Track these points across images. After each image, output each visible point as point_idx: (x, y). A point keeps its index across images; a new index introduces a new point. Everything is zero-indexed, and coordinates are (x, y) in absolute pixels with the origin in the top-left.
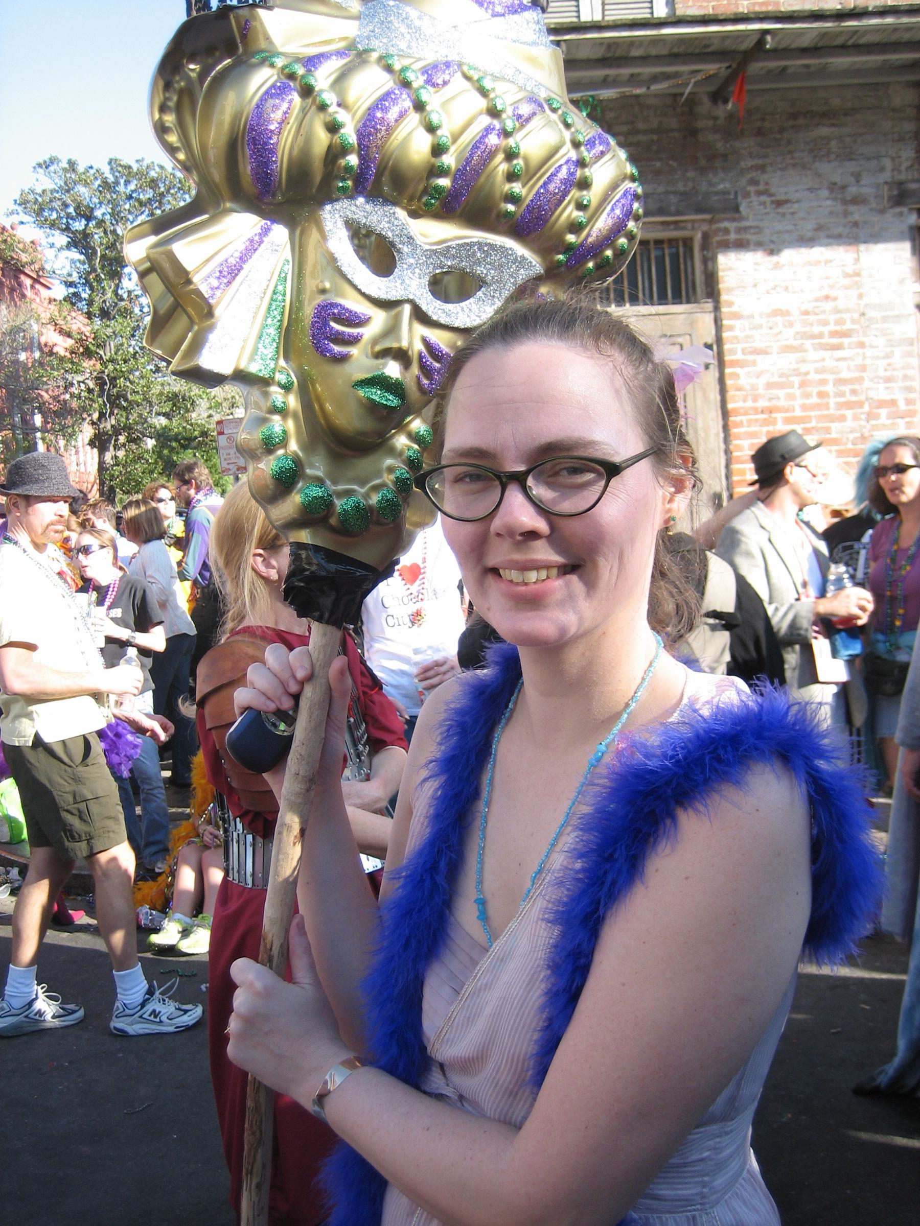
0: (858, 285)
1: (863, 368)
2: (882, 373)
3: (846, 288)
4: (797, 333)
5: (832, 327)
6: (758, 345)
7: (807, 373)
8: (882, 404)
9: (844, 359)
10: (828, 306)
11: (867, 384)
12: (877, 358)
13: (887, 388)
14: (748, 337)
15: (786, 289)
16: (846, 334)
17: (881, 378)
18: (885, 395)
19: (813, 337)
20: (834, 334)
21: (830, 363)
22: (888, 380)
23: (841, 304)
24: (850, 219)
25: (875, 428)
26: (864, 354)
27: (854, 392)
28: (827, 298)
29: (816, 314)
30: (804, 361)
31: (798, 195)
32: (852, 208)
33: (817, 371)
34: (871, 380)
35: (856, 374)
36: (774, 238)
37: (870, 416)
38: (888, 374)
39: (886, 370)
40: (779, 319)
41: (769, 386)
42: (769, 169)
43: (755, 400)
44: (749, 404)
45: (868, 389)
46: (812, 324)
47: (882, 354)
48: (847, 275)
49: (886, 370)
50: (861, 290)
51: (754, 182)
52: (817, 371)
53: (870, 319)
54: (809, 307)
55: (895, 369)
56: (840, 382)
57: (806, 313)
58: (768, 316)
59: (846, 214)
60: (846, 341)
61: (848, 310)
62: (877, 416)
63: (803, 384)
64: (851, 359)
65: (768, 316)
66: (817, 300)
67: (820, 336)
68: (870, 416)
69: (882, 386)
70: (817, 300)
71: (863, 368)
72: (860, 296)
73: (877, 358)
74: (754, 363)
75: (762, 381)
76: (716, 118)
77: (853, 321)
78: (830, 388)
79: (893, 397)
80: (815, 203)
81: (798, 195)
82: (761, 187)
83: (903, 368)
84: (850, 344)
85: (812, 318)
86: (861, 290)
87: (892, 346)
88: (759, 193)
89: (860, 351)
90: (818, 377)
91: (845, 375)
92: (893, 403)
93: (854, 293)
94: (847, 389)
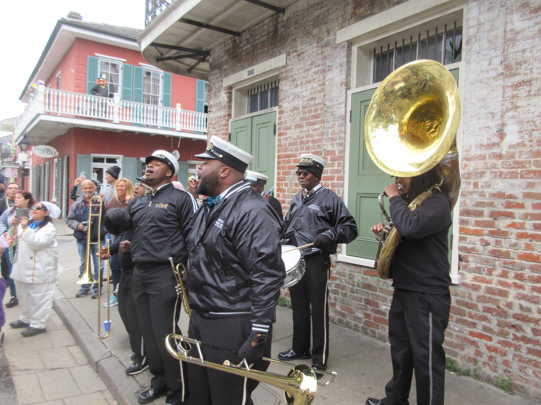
0: (323, 90)
1: (322, 134)
2: (330, 136)
3: (319, 92)
4: (301, 118)
5: (313, 114)
6: (288, 125)
7: (303, 137)
9: (316, 130)
10: (312, 103)
11: (324, 142)
12: (329, 128)
13: (331, 144)
14: (286, 121)
15: (299, 96)
16: (318, 117)
17: (329, 139)
18: (330, 148)
19: (306, 119)
20: (315, 117)
21: (311, 132)
22: (332, 139)
23: (317, 101)
24: (324, 55)
27: (318, 146)
28: (312, 99)
29: (308, 107)
30: (301, 132)
31: (306, 49)
32: (324, 49)
33: (307, 136)
36: (297, 73)
38: (333, 136)
40: (295, 112)
41: (290, 144)
42: (297, 39)
43: (285, 152)
44: (284, 153)
46: (306, 113)
48: (320, 85)
49: (331, 134)
51: (292, 48)
52: (307, 136)
53: (327, 107)
54: (305, 104)
55: (335, 134)
56: (314, 141)
57: (304, 107)
58: (292, 111)
59: (322, 53)
60: (318, 120)
61: (319, 104)
63: (302, 143)
65: (292, 111)
66: (308, 100)
67: (308, 119)
70: (308, 100)
71: (322, 134)
72: (324, 96)
74: (286, 134)
75: (288, 142)
76: (283, 21)
78: (311, 145)
79: (334, 149)
80: (311, 51)
81: (306, 49)
82: (294, 49)
83: (339, 133)
85: (306, 110)
86: (325, 92)
87: (335, 121)
88: (293, 52)
89: (322, 125)
90: (306, 139)
91: (316, 138)
92: (333, 152)
93: (322, 94)
94: (316, 145)
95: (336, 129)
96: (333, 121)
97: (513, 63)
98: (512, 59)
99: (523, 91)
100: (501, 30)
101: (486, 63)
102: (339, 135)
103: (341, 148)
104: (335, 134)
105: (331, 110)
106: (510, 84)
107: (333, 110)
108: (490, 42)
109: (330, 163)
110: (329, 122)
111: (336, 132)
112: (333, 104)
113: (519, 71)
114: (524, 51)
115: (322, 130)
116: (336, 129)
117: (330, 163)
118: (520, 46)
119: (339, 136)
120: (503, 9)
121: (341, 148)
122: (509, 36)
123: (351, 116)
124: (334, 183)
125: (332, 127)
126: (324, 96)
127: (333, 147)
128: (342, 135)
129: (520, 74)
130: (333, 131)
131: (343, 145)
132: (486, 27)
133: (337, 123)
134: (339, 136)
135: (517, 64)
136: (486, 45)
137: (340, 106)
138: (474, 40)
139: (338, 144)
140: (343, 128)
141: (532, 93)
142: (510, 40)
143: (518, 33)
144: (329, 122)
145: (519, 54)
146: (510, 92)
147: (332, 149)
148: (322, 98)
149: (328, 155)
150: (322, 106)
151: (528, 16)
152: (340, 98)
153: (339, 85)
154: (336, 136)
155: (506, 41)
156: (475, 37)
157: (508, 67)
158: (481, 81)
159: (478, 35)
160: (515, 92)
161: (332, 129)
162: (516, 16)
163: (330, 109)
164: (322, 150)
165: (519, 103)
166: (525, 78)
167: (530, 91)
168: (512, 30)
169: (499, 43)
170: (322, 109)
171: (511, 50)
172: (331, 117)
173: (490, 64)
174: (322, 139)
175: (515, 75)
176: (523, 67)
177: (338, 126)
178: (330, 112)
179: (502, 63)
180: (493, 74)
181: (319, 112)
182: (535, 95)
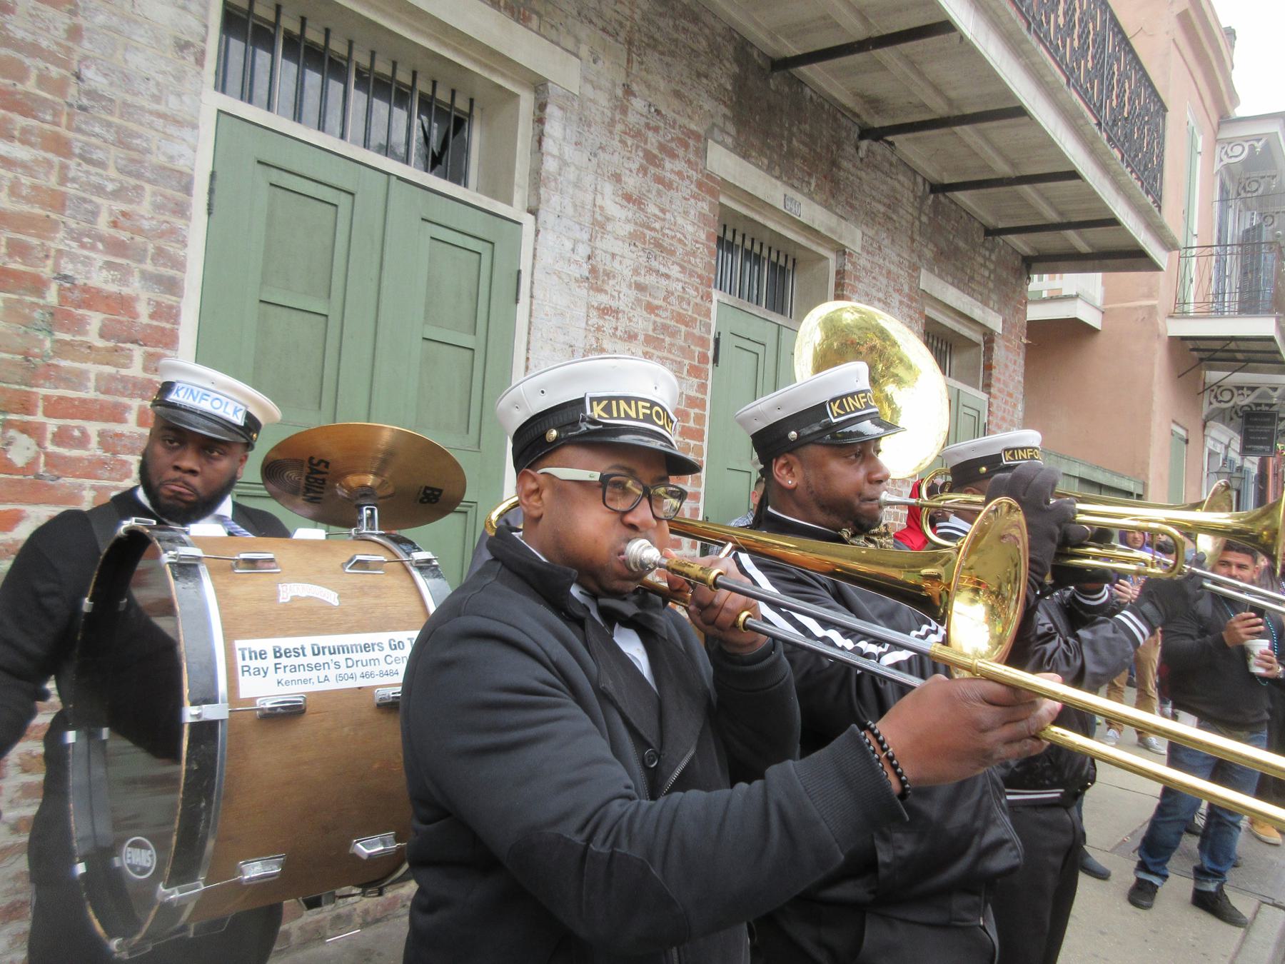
8: (93, 298)
11: (59, 241)
12: (99, 190)
13: (109, 265)
17: (101, 238)
18: (100, 279)
22: (117, 247)
25: (63, 349)
26: (64, 168)
34: (77, 237)
35: (37, 211)
37: (58, 318)
38: (124, 236)
39: (115, 224)
45: (60, 252)
47: (110, 187)
49: (115, 224)
50: (80, 20)
53: (92, 94)
60: (21, 121)
61: (34, 50)
62: (78, 325)
64: (23, 165)
68: (58, 318)
69: (99, 258)
72: (75, 33)
73: (99, 190)
77: (43, 80)
79: (125, 291)
83: (162, 235)
84: (25, 131)
87: (139, 176)
92: (123, 304)
95: (144, 208)
96: (121, 171)
97: (601, 268)
98: (603, 261)
99: (608, 324)
100: (589, 198)
101: (569, 245)
102: (161, 242)
103: (168, 299)
104: (140, 231)
105: (115, 120)
106: (596, 305)
107: (132, 126)
108: (575, 206)
109: (100, 343)
110: (101, 164)
111: (146, 225)
112: (129, 98)
113: (606, 287)
114: (613, 255)
115: (53, 181)
116: (144, 208)
117: (100, 343)
118: (607, 244)
119: (160, 252)
120: (595, 161)
121: (168, 299)
122: (599, 218)
123: (211, 191)
124: (119, 436)
125: (116, 195)
126: (75, 33)
127: (123, 281)
128: (171, 248)
129: (606, 292)
130: (124, 214)
131: (173, 286)
132: (571, 174)
133: (148, 188)
134: (160, 252)
135: (604, 270)
136: (570, 210)
137: (172, 130)
138: (553, 184)
139: (145, 276)
140: (179, 223)
141: (619, 333)
142: (600, 225)
143: (608, 219)
144: (101, 164)
145: (609, 257)
146: (594, 320)
147: (113, 288)
148: (61, 34)
149: (87, 304)
150: (55, 72)
151: (618, 199)
152: (173, 102)
153: (169, 41)
154: (138, 239)
155: (595, 223)
156: (556, 180)
157: (593, 270)
158: (559, 275)
159: (561, 179)
160: (601, 322)
161: (118, 206)
162: (608, 188)
163: (111, 113)
164: (46, 271)
165: (607, 344)
166: (614, 304)
167: (616, 329)
168: (601, 208)
169: (587, 219)
170: (59, 87)
171: (598, 244)
172: (114, 155)
173: (573, 250)
174: (52, 226)
175: (600, 290)
176: (612, 282)
177: (158, 207)
178: (109, 125)
179: (589, 258)
180: (576, 272)
181: (30, 86)
182: (621, 338)
